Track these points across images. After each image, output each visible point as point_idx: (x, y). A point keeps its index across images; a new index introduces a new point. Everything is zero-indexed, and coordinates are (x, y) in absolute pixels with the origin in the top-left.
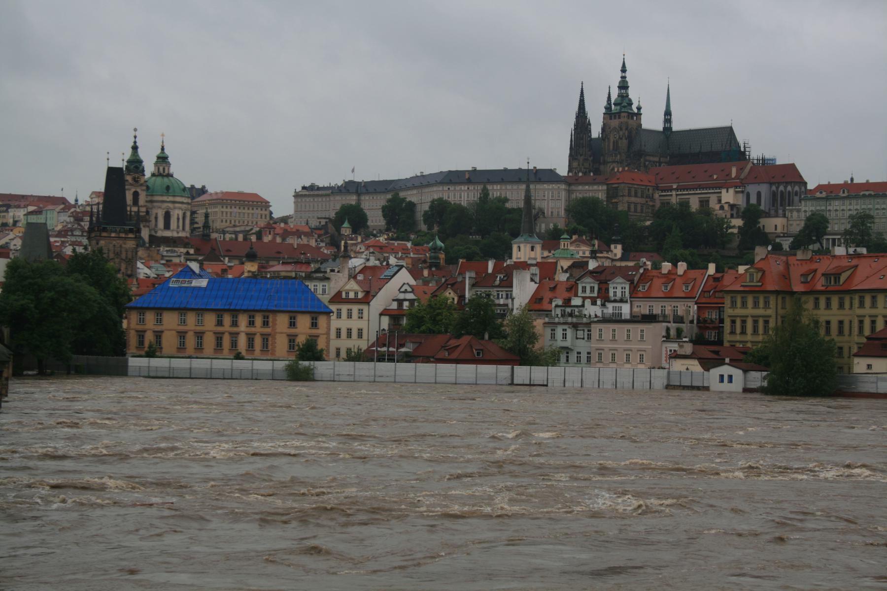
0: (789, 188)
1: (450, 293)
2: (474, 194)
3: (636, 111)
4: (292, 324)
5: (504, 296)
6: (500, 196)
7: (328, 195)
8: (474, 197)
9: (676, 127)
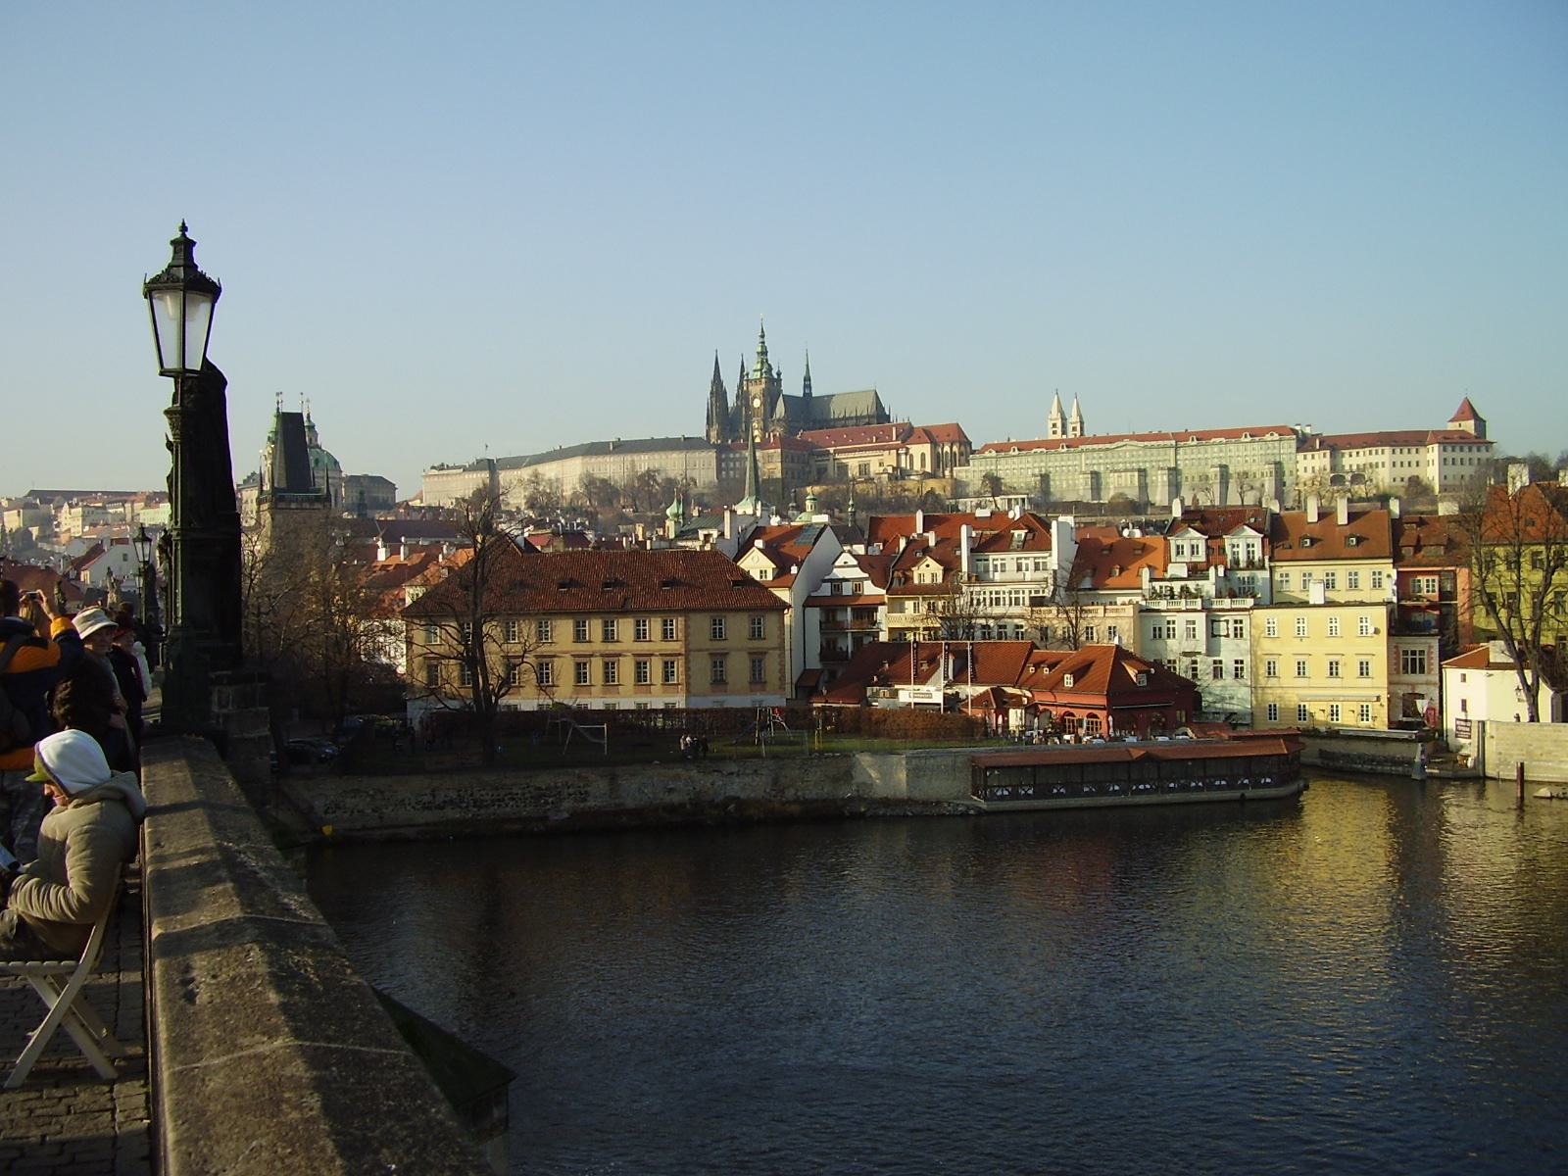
0: (955, 449)
1: (928, 566)
3: (776, 376)
4: (717, 635)
5: (1032, 567)
7: (460, 474)
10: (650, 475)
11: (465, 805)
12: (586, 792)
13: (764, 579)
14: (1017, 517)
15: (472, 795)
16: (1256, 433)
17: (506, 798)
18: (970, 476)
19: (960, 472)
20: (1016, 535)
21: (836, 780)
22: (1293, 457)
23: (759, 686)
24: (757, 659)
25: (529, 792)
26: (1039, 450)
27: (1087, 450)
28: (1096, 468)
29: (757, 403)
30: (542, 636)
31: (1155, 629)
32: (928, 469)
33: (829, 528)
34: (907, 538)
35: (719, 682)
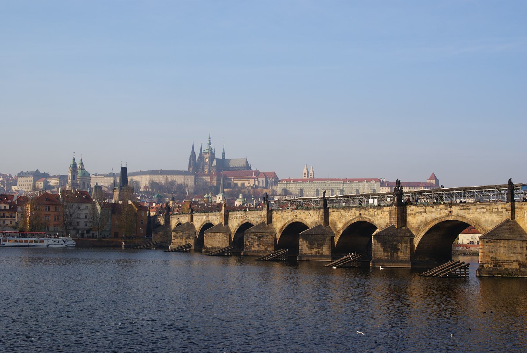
0: (273, 180)
3: (213, 152)
7: (103, 177)
8: (162, 180)
10: (173, 182)
16: (368, 180)
18: (278, 188)
19: (275, 187)
22: (379, 188)
26: (300, 182)
29: (207, 160)
32: (264, 185)
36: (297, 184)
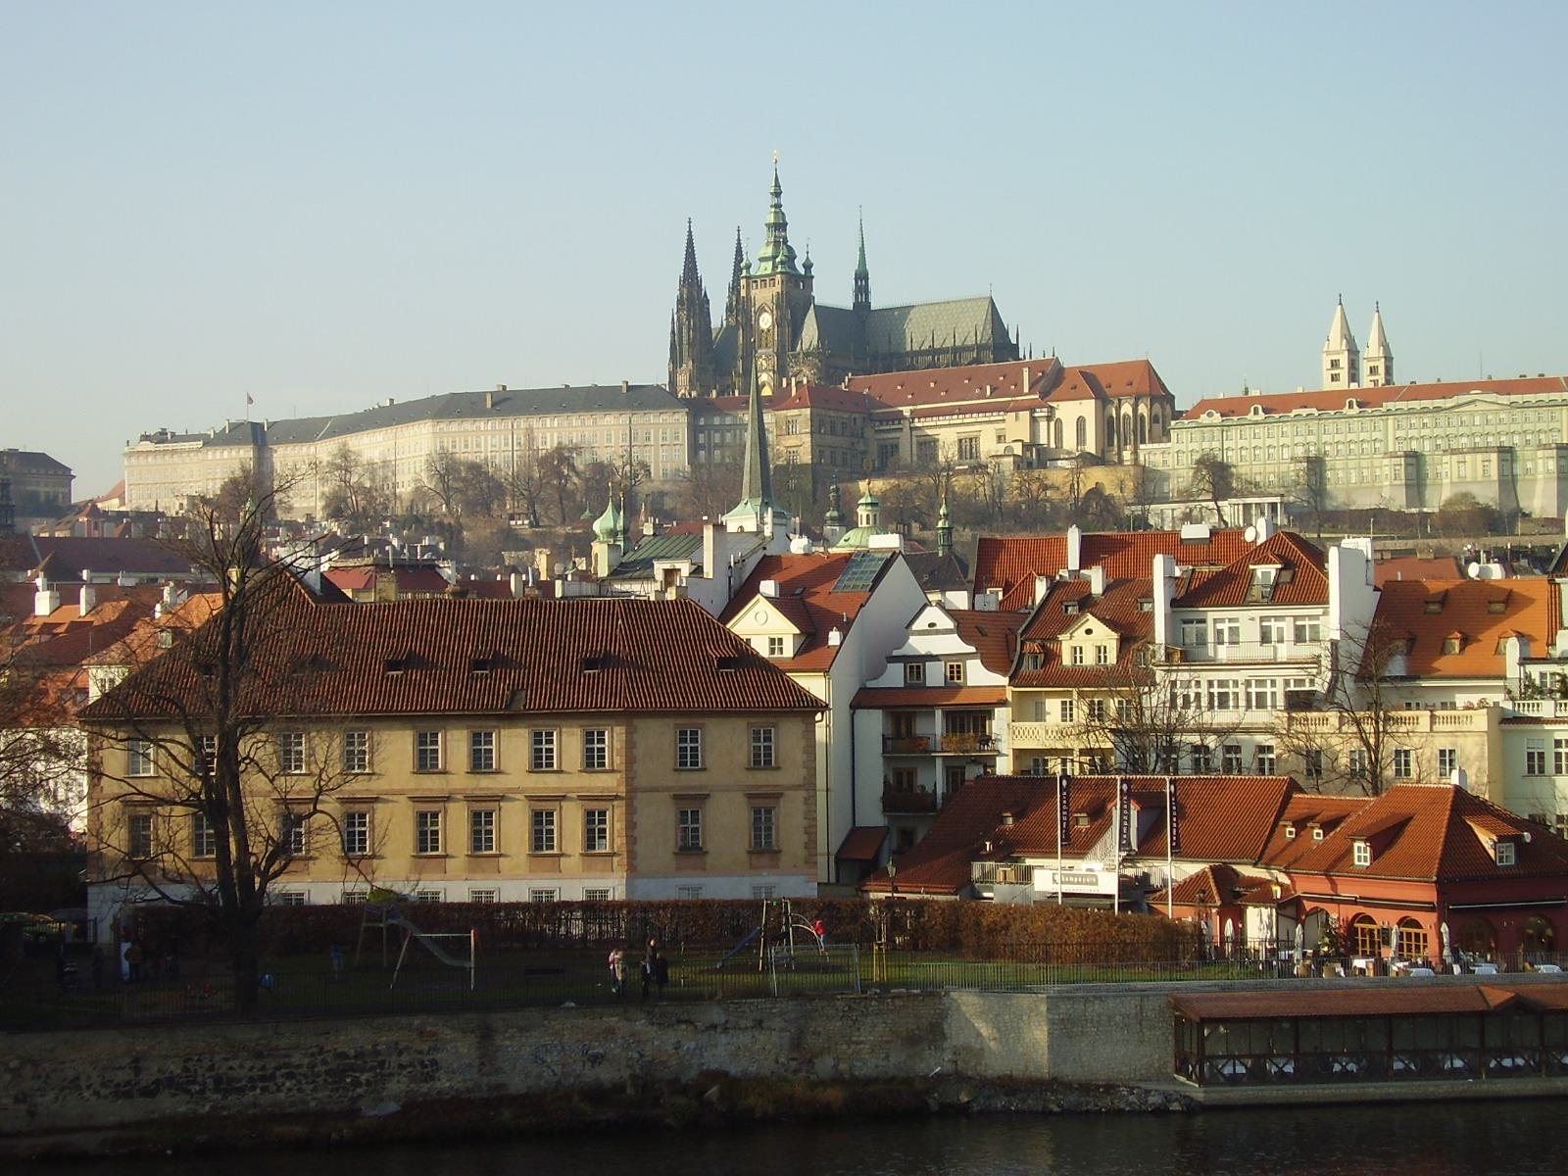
0: (1143, 409)
2: (506, 439)
3: (802, 271)
4: (688, 759)
5: (1289, 635)
6: (559, 443)
7: (198, 450)
8: (506, 445)
9: (877, 302)
10: (561, 457)
11: (198, 1088)
12: (434, 1062)
13: (777, 655)
14: (1262, 539)
15: (211, 1068)
17: (278, 1073)
18: (1171, 460)
19: (1152, 454)
20: (1259, 574)
21: (912, 1040)
23: (765, 860)
24: (763, 808)
25: (325, 1062)
26: (1304, 412)
27: (1398, 413)
28: (1414, 446)
29: (766, 321)
30: (353, 760)
31: (1531, 756)
32: (1091, 447)
33: (900, 561)
34: (1050, 578)
35: (691, 849)
36: (1287, 428)
